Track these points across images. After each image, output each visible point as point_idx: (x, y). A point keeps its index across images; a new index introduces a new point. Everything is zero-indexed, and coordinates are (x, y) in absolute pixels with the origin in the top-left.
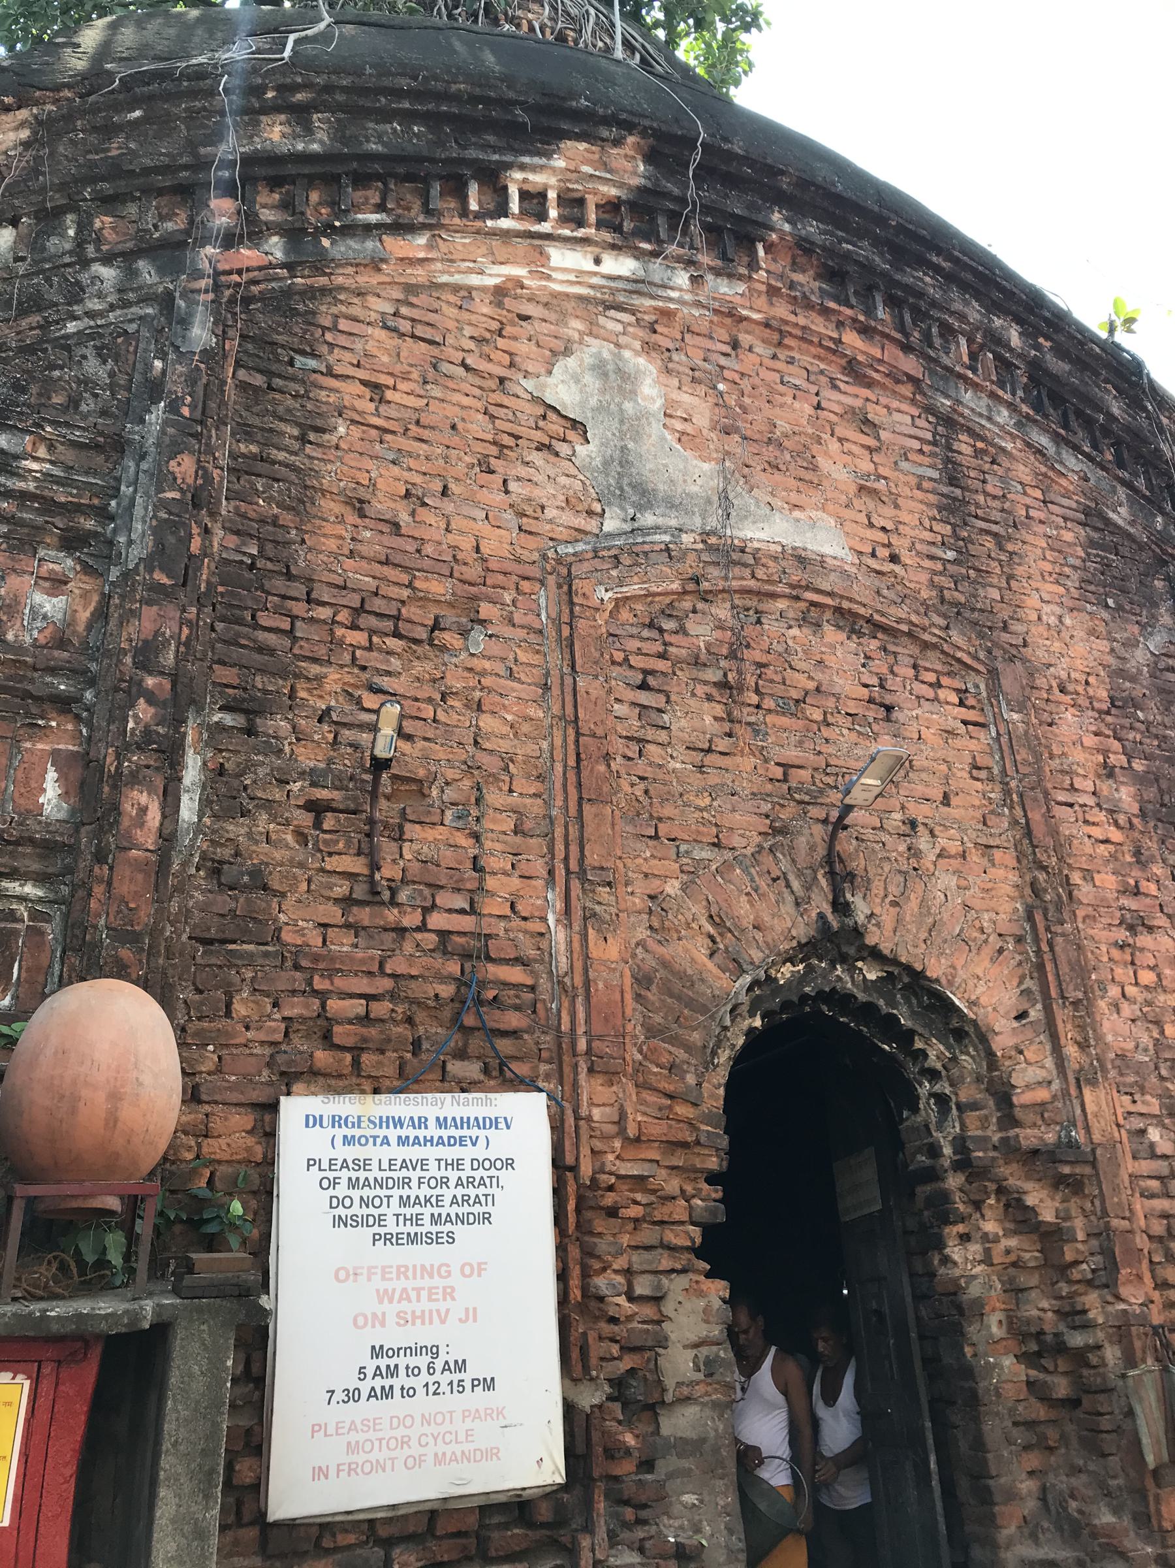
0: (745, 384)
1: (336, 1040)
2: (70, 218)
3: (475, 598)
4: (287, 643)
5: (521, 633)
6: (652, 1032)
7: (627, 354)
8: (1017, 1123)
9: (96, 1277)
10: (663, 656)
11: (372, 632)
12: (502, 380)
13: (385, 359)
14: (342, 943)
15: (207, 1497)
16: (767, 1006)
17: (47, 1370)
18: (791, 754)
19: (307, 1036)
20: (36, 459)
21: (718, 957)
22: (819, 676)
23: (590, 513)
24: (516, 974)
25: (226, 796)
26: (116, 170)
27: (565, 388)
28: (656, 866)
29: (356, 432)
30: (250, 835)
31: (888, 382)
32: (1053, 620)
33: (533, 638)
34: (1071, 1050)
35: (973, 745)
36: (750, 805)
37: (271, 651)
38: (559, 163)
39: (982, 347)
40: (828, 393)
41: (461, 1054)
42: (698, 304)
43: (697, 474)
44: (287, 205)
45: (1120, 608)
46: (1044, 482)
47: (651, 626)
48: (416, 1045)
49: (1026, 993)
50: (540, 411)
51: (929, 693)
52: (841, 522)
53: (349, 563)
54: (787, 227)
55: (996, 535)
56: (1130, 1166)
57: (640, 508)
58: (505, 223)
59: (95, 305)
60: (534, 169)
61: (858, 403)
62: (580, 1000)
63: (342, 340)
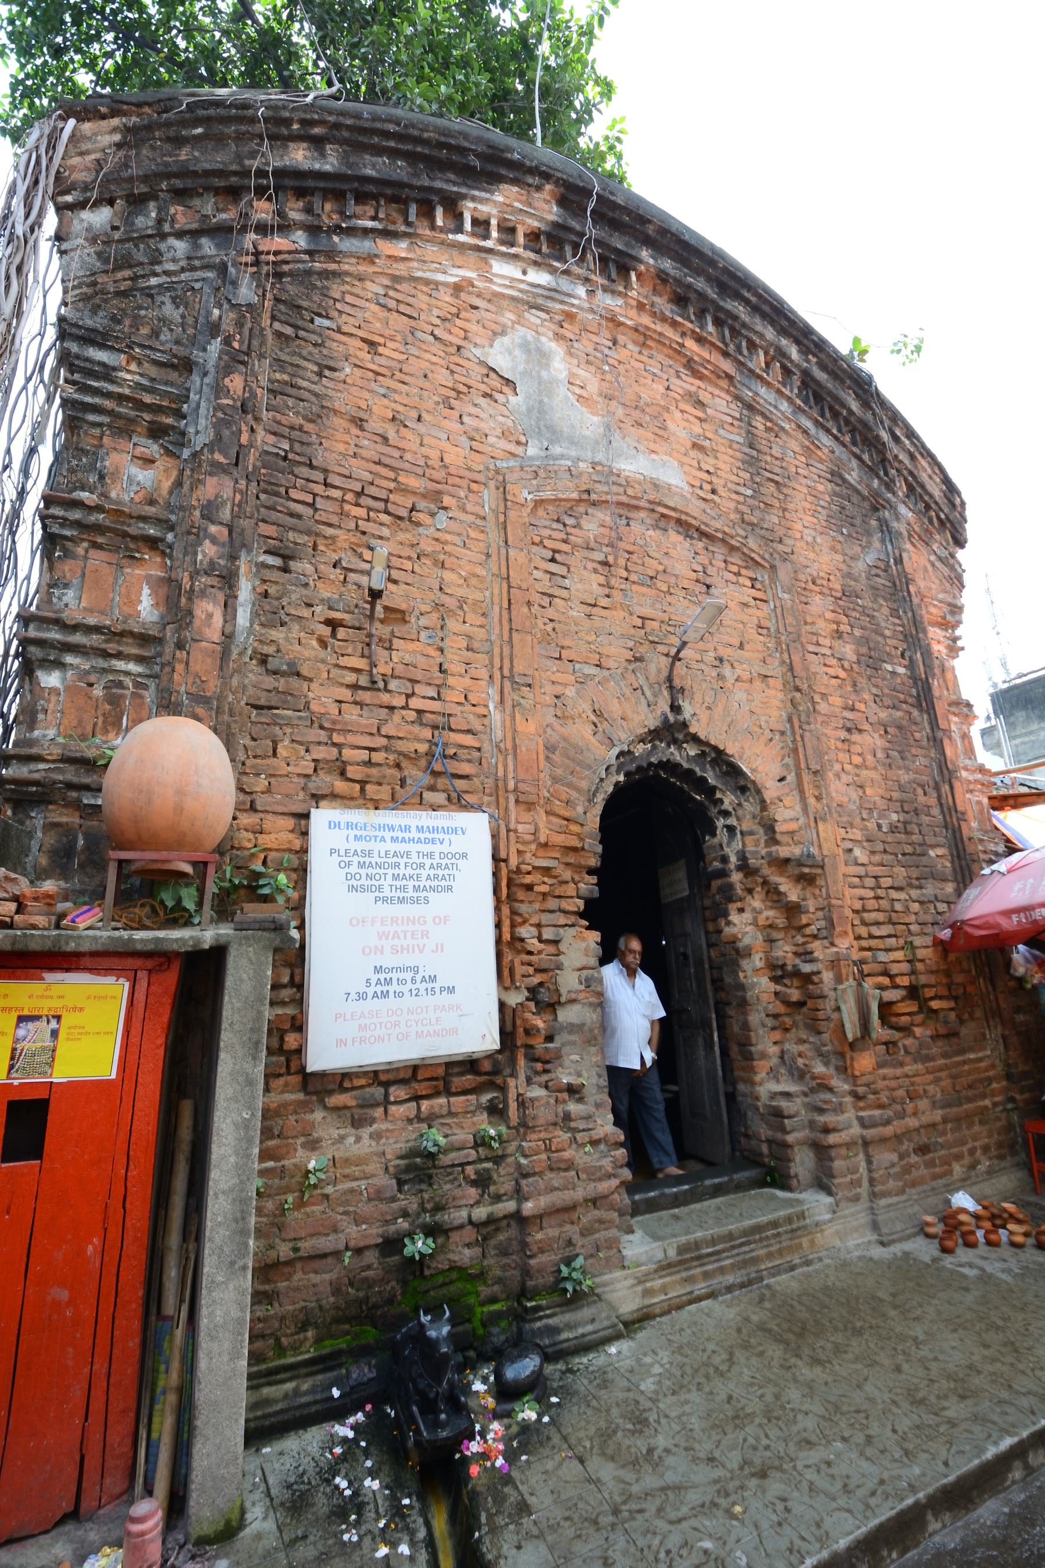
0: (621, 368)
1: (349, 775)
2: (152, 205)
3: (439, 493)
4: (310, 511)
5: (471, 518)
6: (555, 779)
7: (544, 339)
8: (777, 842)
9: (178, 917)
10: (565, 541)
11: (369, 509)
12: (459, 348)
13: (378, 325)
14: (352, 714)
15: (254, 1058)
16: (627, 768)
17: (142, 975)
18: (647, 612)
19: (329, 772)
20: (129, 371)
21: (599, 735)
22: (665, 561)
23: (518, 443)
24: (468, 740)
25: (270, 611)
26: (184, 173)
27: (502, 356)
28: (559, 677)
29: (358, 372)
30: (287, 639)
31: (712, 377)
32: (810, 539)
33: (479, 522)
34: (811, 801)
35: (759, 613)
36: (621, 642)
37: (299, 517)
38: (499, 198)
39: (773, 358)
40: (674, 380)
41: (432, 788)
42: (592, 310)
43: (589, 423)
44: (308, 210)
45: (850, 535)
46: (808, 452)
47: (558, 521)
48: (403, 782)
49: (787, 766)
50: (485, 371)
51: (734, 579)
52: (682, 464)
53: (353, 461)
54: (651, 261)
55: (777, 483)
56: (843, 869)
57: (551, 442)
58: (461, 238)
59: (170, 267)
60: (481, 201)
61: (693, 389)
62: (510, 758)
63: (348, 309)
